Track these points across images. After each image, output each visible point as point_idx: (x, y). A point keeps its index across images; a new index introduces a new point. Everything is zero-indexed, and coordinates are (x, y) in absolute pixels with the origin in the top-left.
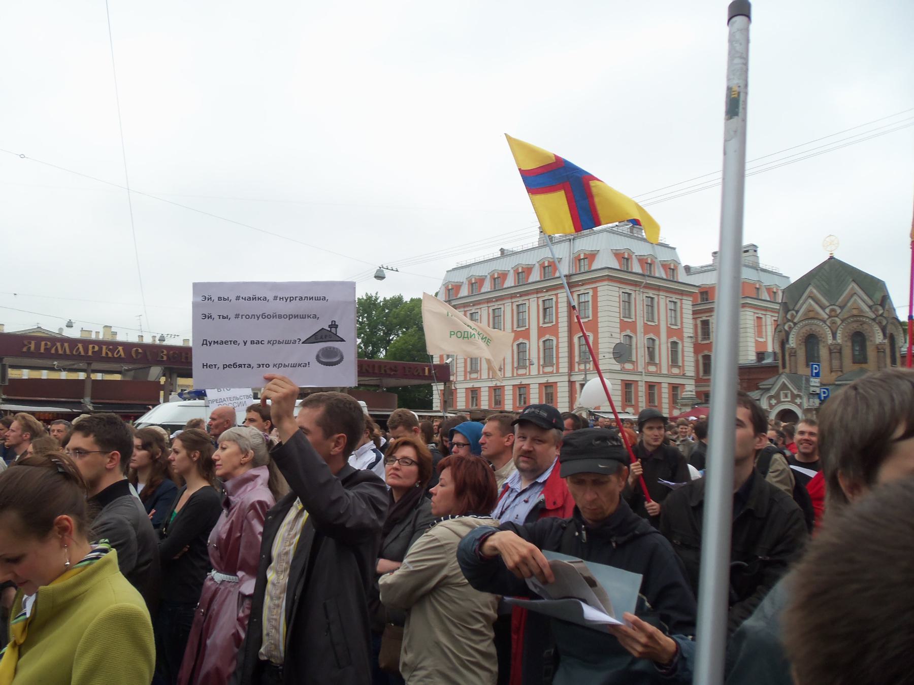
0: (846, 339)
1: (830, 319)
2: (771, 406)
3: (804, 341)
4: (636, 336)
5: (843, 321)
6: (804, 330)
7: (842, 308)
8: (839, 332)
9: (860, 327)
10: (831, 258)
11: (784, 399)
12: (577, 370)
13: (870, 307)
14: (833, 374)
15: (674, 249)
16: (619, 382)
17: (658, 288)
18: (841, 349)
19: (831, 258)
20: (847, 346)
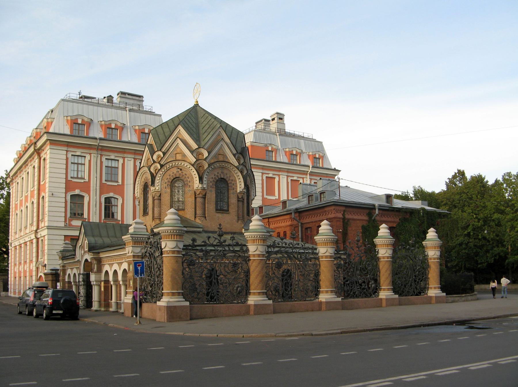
0: (165, 185)
1: (153, 166)
2: (82, 256)
3: (143, 189)
4: (89, 195)
5: (162, 166)
6: (143, 180)
7: (164, 154)
8: (157, 178)
9: (180, 172)
10: (197, 105)
11: (86, 249)
12: (40, 228)
13: (192, 152)
14: (153, 222)
15: (160, 115)
16: (63, 238)
17: (123, 151)
18: (160, 196)
19: (197, 105)
20: (166, 193)
